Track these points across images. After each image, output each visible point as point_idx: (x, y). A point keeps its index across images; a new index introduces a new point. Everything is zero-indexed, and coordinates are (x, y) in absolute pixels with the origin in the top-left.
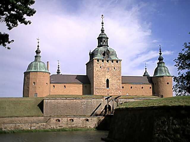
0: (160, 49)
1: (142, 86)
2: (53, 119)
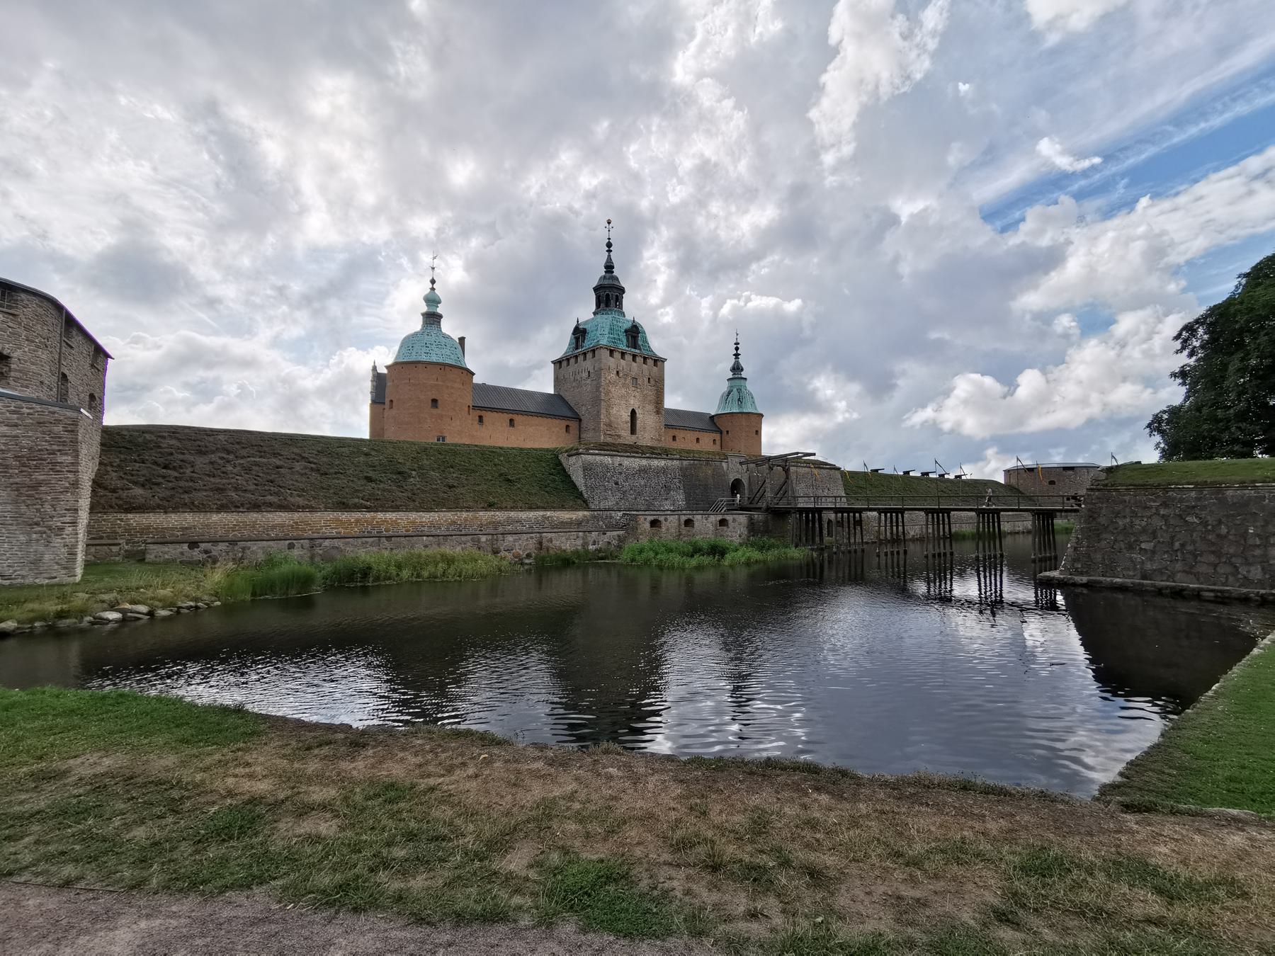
1: (697, 434)
2: (642, 518)
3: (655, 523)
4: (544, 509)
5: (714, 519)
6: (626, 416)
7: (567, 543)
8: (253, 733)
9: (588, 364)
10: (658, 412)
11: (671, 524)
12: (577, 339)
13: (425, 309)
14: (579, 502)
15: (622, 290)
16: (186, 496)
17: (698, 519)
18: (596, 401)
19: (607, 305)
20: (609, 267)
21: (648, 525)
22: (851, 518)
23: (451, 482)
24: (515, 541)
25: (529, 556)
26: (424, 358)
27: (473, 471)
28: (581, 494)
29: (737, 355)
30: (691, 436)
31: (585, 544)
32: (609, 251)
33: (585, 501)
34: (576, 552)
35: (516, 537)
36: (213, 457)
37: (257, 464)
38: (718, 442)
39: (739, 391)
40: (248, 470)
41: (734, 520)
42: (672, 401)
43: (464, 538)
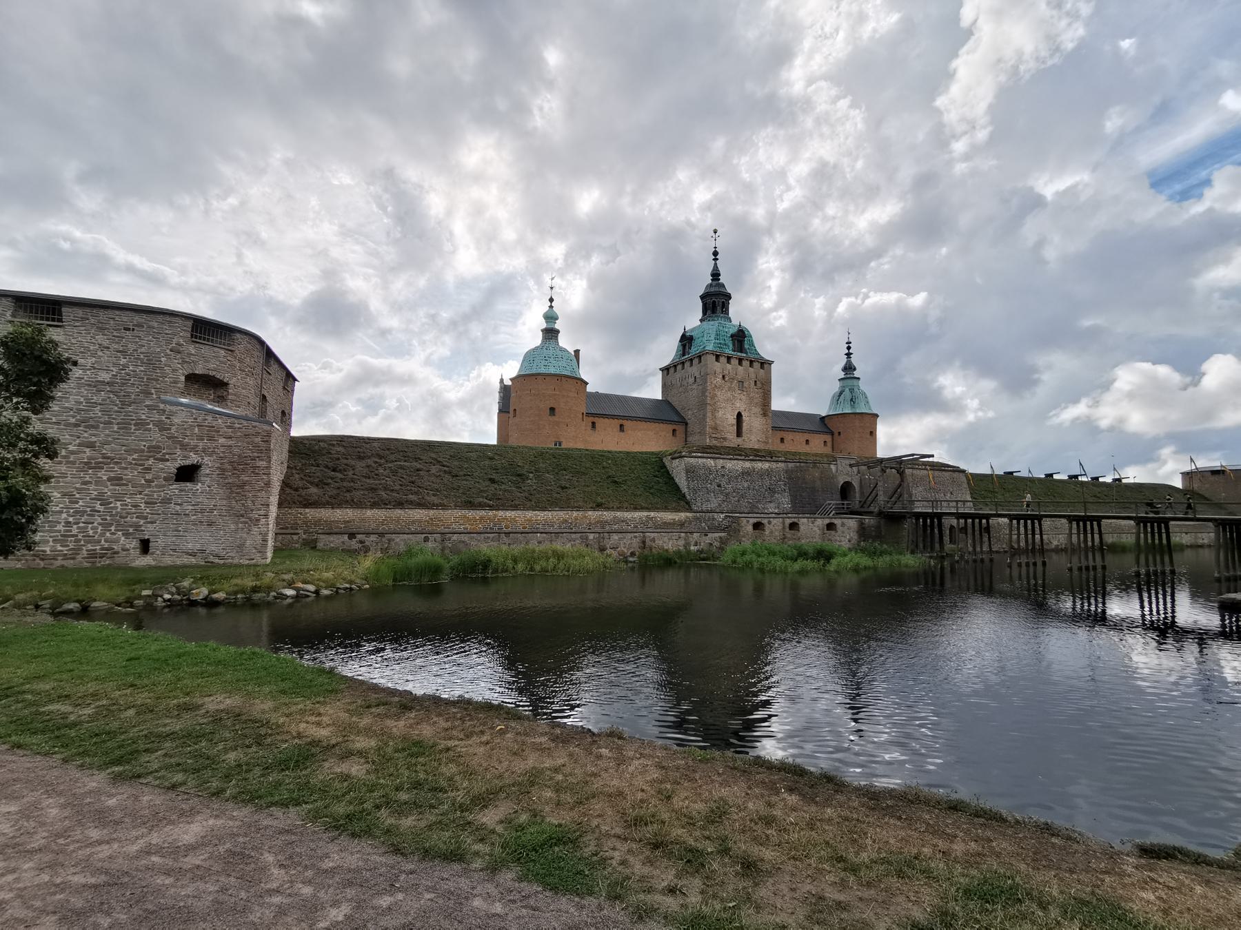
0: (849, 343)
1: (807, 436)
2: (744, 520)
3: (758, 526)
4: (648, 509)
5: (821, 522)
6: (732, 420)
7: (670, 543)
8: (331, 691)
9: (694, 370)
10: (764, 415)
11: (775, 527)
12: (684, 346)
13: (544, 325)
14: (682, 503)
15: (729, 297)
16: (348, 495)
17: (803, 522)
18: (702, 405)
19: (714, 312)
20: (716, 275)
21: (750, 528)
22: (977, 524)
23: (563, 483)
24: (620, 539)
25: (633, 554)
26: (543, 370)
27: (584, 474)
28: (684, 496)
29: (849, 355)
30: (801, 438)
31: (687, 545)
32: (716, 259)
33: (688, 503)
34: (678, 553)
35: (621, 535)
36: (370, 462)
37: (402, 467)
38: (829, 444)
39: (852, 391)
40: (394, 472)
41: (843, 525)
42: (779, 403)
43: (573, 536)
